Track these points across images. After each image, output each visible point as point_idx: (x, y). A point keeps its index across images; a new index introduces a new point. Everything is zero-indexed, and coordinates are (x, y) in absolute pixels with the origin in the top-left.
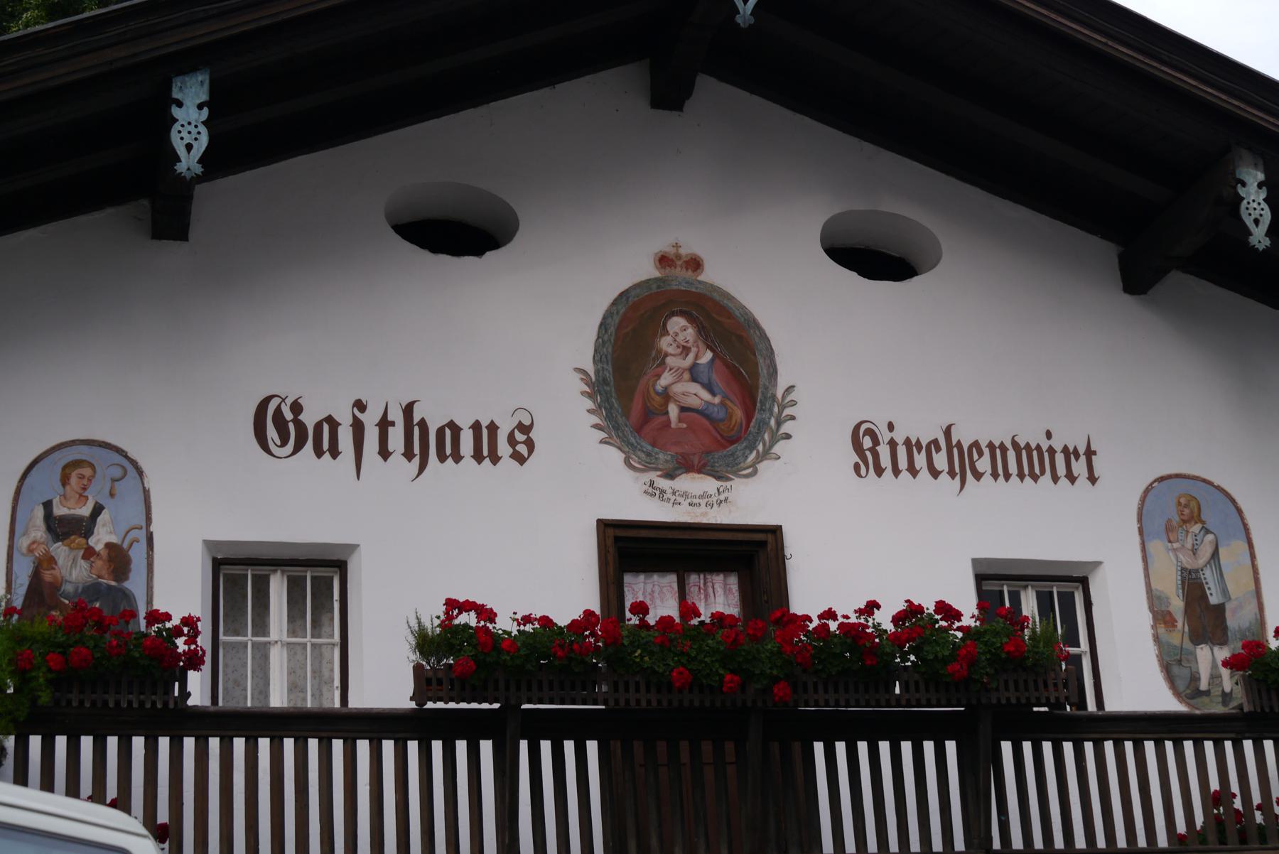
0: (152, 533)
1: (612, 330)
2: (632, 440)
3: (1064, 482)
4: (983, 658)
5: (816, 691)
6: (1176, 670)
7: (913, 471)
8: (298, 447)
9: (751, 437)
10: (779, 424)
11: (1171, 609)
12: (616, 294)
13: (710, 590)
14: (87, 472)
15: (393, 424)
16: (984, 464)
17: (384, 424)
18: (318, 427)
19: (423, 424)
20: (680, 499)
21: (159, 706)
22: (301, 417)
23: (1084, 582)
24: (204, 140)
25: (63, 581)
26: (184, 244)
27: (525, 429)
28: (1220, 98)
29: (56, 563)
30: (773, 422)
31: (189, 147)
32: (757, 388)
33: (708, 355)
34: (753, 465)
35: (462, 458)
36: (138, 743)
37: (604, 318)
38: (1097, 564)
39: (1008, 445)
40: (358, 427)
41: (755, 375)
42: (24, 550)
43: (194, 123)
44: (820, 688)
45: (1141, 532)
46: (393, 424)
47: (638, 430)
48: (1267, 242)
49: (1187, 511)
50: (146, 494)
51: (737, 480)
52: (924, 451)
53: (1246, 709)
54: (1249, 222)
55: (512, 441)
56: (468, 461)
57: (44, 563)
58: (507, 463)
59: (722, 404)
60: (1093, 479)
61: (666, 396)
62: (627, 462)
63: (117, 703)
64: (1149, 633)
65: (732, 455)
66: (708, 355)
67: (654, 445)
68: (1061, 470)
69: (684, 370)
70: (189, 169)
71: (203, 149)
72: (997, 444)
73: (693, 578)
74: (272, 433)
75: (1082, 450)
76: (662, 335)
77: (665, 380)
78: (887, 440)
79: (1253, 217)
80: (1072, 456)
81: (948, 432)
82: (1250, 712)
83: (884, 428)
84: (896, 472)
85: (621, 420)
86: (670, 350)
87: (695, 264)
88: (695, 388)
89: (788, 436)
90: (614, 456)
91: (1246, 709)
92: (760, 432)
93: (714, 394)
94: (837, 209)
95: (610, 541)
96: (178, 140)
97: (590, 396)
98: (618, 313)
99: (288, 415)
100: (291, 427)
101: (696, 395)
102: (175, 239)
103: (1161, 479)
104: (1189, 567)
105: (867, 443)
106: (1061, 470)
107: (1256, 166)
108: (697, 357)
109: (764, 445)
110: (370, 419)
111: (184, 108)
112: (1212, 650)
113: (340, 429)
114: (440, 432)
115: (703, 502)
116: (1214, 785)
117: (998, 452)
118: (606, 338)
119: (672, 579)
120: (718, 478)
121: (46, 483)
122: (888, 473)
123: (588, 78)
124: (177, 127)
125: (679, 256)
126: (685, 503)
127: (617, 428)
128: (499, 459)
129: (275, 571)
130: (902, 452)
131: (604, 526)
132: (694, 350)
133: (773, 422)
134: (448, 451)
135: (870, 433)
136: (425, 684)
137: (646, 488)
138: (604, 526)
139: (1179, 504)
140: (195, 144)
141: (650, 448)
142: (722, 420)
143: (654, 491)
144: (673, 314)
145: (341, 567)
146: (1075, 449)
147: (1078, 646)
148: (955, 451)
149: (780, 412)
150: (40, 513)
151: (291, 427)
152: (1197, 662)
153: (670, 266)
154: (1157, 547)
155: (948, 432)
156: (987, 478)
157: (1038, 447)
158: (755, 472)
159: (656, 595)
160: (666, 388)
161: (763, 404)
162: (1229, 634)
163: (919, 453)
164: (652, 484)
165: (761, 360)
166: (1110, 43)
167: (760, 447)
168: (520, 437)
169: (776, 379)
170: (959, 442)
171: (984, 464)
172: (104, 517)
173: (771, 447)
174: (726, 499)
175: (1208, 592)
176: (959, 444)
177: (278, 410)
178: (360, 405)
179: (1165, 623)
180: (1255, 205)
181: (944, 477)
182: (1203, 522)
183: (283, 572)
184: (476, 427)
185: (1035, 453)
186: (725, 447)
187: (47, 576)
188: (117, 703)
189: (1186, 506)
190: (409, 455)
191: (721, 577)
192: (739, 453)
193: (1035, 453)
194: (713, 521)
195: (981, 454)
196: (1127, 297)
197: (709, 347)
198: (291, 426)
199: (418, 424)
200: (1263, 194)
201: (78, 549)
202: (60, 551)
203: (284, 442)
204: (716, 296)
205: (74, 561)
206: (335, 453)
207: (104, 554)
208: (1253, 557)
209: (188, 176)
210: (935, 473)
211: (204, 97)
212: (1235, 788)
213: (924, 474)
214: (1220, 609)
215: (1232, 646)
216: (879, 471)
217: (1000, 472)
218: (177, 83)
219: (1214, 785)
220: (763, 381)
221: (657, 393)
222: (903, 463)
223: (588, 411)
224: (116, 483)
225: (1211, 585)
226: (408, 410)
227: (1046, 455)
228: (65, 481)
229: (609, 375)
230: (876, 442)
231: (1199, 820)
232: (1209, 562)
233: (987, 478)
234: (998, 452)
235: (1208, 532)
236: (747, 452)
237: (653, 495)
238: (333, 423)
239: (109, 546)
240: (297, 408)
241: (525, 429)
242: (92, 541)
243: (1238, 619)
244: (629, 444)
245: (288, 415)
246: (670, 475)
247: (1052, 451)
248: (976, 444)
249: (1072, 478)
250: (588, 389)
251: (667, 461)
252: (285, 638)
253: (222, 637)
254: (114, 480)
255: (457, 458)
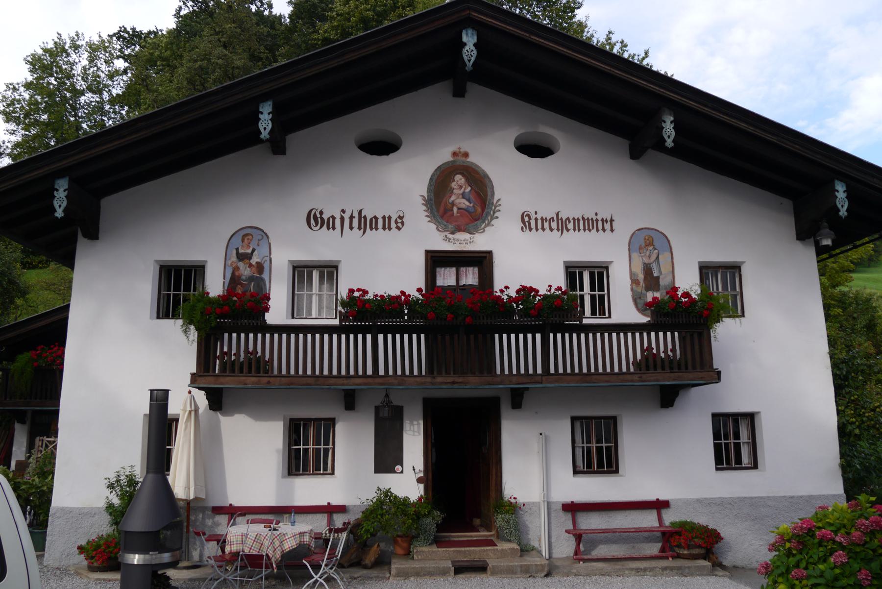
0: (271, 258)
1: (434, 181)
2: (440, 221)
3: (601, 232)
4: (546, 307)
5: (483, 319)
6: (638, 301)
7: (543, 229)
8: (321, 227)
9: (483, 219)
10: (494, 213)
11: (638, 278)
12: (436, 167)
13: (468, 273)
14: (250, 237)
15: (354, 217)
16: (570, 226)
17: (352, 218)
18: (329, 219)
19: (365, 217)
20: (456, 242)
21: (255, 324)
22: (322, 216)
23: (607, 268)
24: (270, 126)
25: (242, 275)
26: (285, 156)
27: (401, 218)
28: (656, 89)
29: (239, 269)
30: (492, 213)
31: (265, 129)
32: (487, 200)
33: (469, 188)
34: (484, 228)
35: (378, 229)
36: (251, 335)
37: (432, 176)
38: (611, 262)
39: (581, 218)
40: (342, 219)
41: (486, 195)
42: (229, 265)
43: (267, 120)
44: (485, 317)
45: (629, 250)
46: (354, 217)
47: (442, 217)
48: (672, 144)
49: (648, 242)
50: (270, 244)
51: (477, 234)
52: (548, 222)
53: (651, 322)
54: (666, 137)
55: (396, 222)
56: (380, 230)
57: (236, 269)
58: (394, 230)
59: (473, 206)
60: (612, 230)
61: (453, 204)
62: (437, 229)
63: (241, 324)
64: (629, 287)
65: (476, 225)
66: (469, 188)
67: (447, 222)
68: (600, 227)
69: (460, 194)
70: (265, 137)
71: (270, 129)
72: (576, 218)
73: (463, 269)
74: (312, 222)
75: (609, 219)
76: (452, 182)
77: (452, 199)
78: (534, 218)
79: (668, 135)
80: (605, 222)
81: (557, 215)
82: (652, 324)
83: (533, 213)
84: (537, 229)
85: (436, 214)
86: (455, 187)
87: (466, 155)
88: (464, 201)
89: (497, 218)
90: (433, 226)
91: (651, 322)
92: (487, 216)
93: (470, 203)
94: (522, 131)
95: (429, 258)
96: (56, 204)
97: (425, 205)
98: (437, 174)
99: (318, 216)
100: (319, 219)
101: (464, 203)
102: (282, 154)
103: (639, 230)
104: (647, 263)
105: (527, 219)
106: (600, 227)
107: (670, 115)
108: (465, 189)
109: (488, 221)
110: (347, 216)
111: (263, 115)
112: (410, 427)
113: (336, 220)
114: (371, 220)
115: (464, 243)
116: (646, 345)
117: (576, 221)
118: (432, 183)
119: (454, 269)
120: (470, 233)
121: (237, 241)
122: (534, 230)
123: (430, 87)
124: (261, 121)
125: (460, 152)
126: (458, 243)
127: (434, 216)
128: (391, 229)
129: (314, 269)
130: (539, 222)
131: (427, 252)
132: (464, 187)
133: (492, 213)
134: (374, 226)
135: (528, 216)
136: (343, 317)
137: (443, 238)
138: (427, 252)
139: (645, 239)
140: (267, 127)
141: (446, 223)
142: (473, 212)
143: (447, 239)
144: (457, 174)
145: (336, 267)
146: (606, 219)
147: (604, 292)
148: (560, 221)
149: (495, 209)
150: (234, 252)
151: (319, 219)
152: (647, 298)
153: (457, 156)
154: (635, 255)
155: (557, 215)
156: (572, 231)
157: (592, 219)
158: (484, 231)
159: (448, 275)
160: (453, 201)
161: (488, 206)
162: (660, 287)
163: (546, 222)
164: (446, 236)
165: (488, 190)
166: (612, 69)
167: (487, 222)
168: (399, 221)
169: (494, 197)
170: (562, 218)
171: (570, 226)
172: (256, 253)
173: (491, 221)
174: (473, 241)
175: (653, 272)
176: (562, 219)
177: (315, 214)
178: (343, 211)
179: (636, 283)
180: (669, 130)
181: (555, 231)
182: (654, 246)
183: (317, 270)
184: (384, 218)
185: (590, 221)
186: (473, 222)
187: (237, 273)
188: (241, 324)
189: (648, 240)
190: (360, 228)
191: (472, 268)
192: (479, 224)
193: (590, 221)
194: (467, 250)
195: (570, 222)
196: (631, 160)
197: (469, 186)
198: (319, 219)
199: (363, 217)
200: (672, 126)
201: (247, 264)
202: (241, 265)
203: (317, 225)
204: (474, 167)
205: (246, 268)
206: (334, 228)
207: (255, 266)
208: (672, 258)
209: (264, 139)
210: (551, 230)
211: (270, 110)
212: (654, 345)
213: (548, 230)
214: (658, 278)
215: (661, 292)
216: (530, 229)
217: (576, 229)
218: (261, 105)
219: (646, 345)
220: (489, 197)
221: (450, 203)
222: (540, 226)
223: (424, 210)
224: (260, 241)
225: (655, 269)
226: (360, 212)
227: (595, 222)
228: (243, 241)
229: (432, 197)
230: (530, 219)
231: (639, 356)
232: (655, 261)
233: (572, 231)
234: (576, 221)
235: (655, 249)
236: (482, 224)
237: (446, 240)
238: (333, 218)
239: (257, 263)
240: (321, 213)
241: (401, 218)
242: (251, 261)
243: (664, 282)
244: (439, 222)
245: (318, 216)
246: (453, 233)
247: (597, 220)
248: (568, 219)
249: (604, 230)
250: (424, 203)
251: (452, 228)
252: (318, 293)
253: (296, 292)
254: (259, 240)
255: (377, 229)
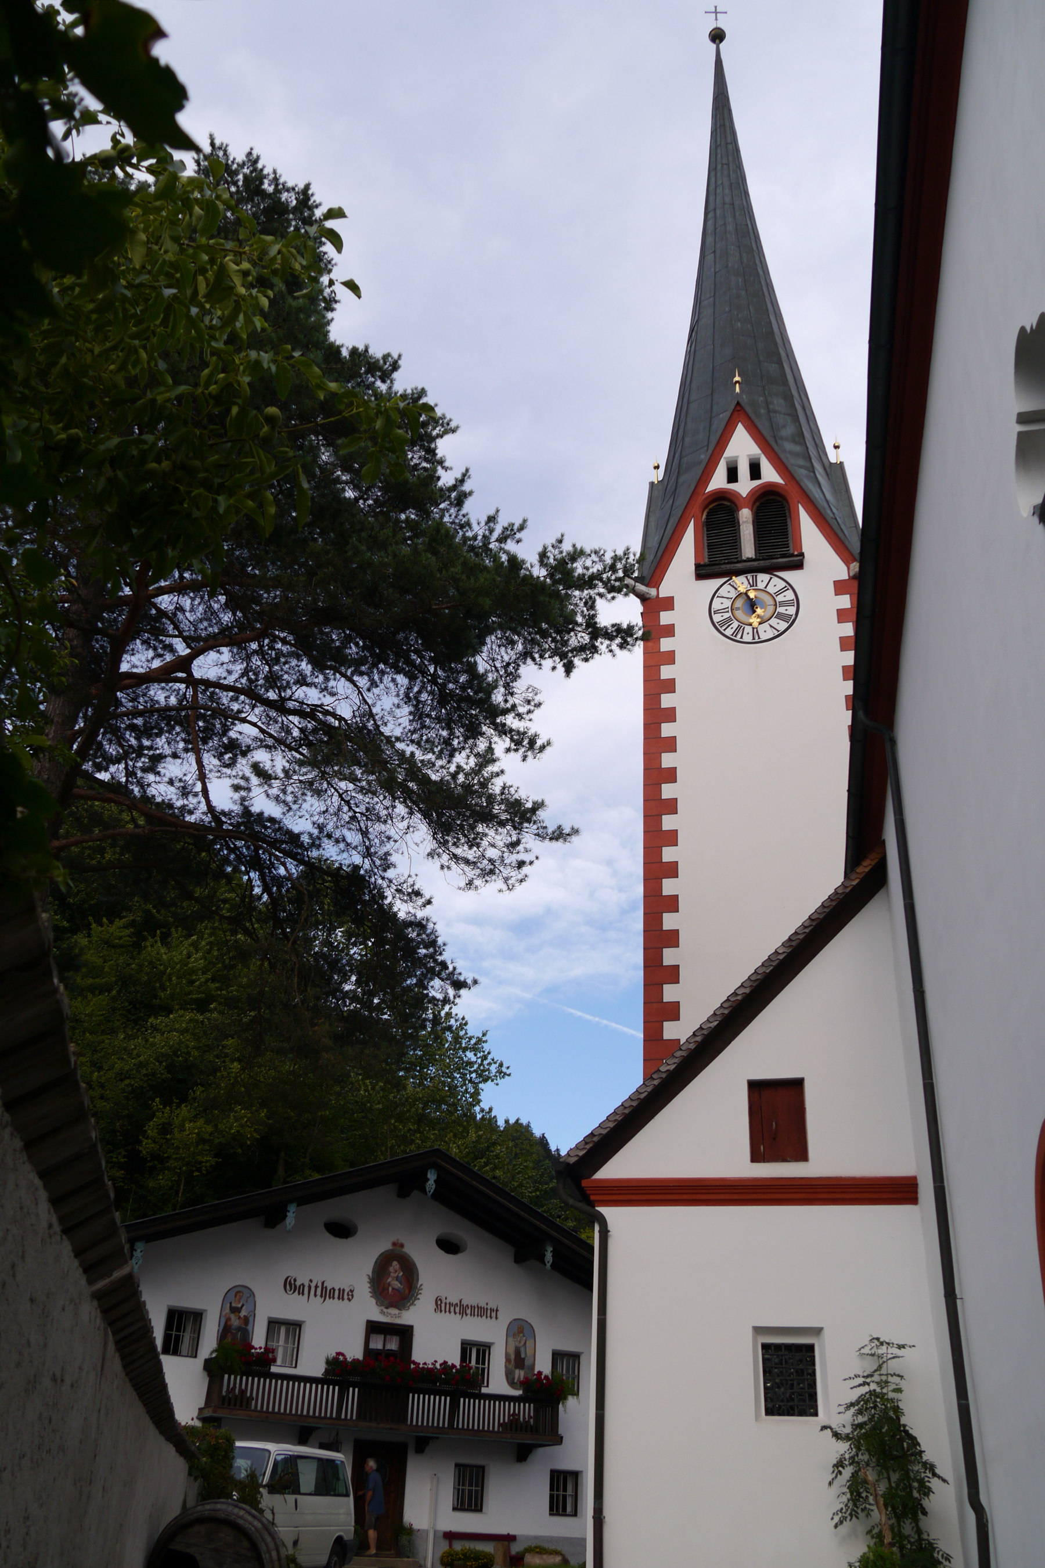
7: (450, 1312)
16: (468, 1312)
17: (316, 1287)
19: (326, 1288)
27: (352, 1291)
38: (493, 1343)
55: (348, 1294)
57: (228, 1319)
58: (346, 1300)
60: (496, 1318)
61: (389, 1285)
68: (489, 1315)
73: (388, 1337)
74: (288, 1287)
81: (461, 1301)
90: (373, 1301)
101: (397, 1285)
103: (515, 1320)
105: (439, 1302)
106: (489, 1315)
110: (313, 1285)
116: (512, 1412)
119: (383, 1336)
135: (440, 1300)
143: (382, 1312)
154: (510, 1339)
155: (461, 1301)
171: (468, 1312)
172: (244, 1308)
187: (229, 1323)
190: (321, 1296)
202: (233, 1316)
206: (303, 1294)
210: (455, 1313)
213: (453, 1313)
214: (524, 1359)
217: (472, 1314)
219: (512, 1412)
226: (323, 1283)
228: (236, 1296)
231: (506, 1420)
240: (295, 1280)
243: (527, 1363)
248: (467, 1305)
249: (491, 1317)
255: (334, 1298)
